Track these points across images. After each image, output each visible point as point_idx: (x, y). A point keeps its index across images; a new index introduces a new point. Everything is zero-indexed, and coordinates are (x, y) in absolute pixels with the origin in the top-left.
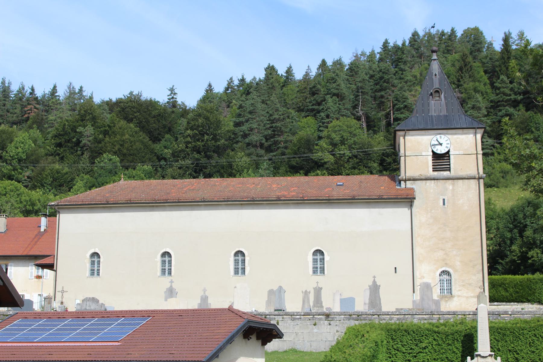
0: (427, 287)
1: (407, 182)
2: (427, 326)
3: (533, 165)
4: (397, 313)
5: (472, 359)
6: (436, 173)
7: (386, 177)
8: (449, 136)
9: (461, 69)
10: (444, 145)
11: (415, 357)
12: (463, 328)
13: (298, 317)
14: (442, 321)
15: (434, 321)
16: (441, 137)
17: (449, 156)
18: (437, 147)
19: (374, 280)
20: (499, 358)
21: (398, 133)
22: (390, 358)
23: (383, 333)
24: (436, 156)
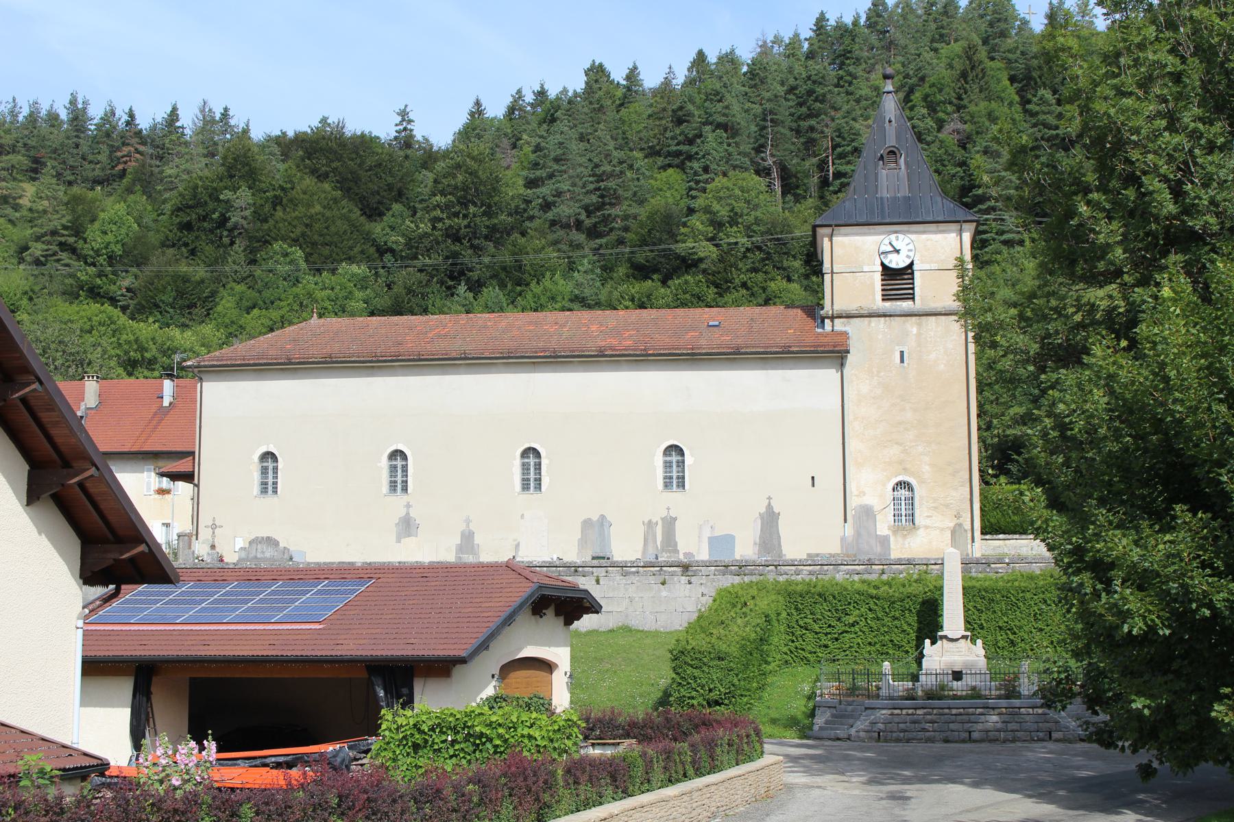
0: (867, 513)
1: (836, 321)
2: (857, 586)
3: (998, 338)
4: (809, 562)
5: (933, 643)
6: (888, 304)
7: (799, 311)
8: (913, 237)
9: (964, 75)
10: (903, 253)
11: (837, 639)
12: (921, 589)
13: (633, 569)
14: (885, 577)
15: (873, 577)
16: (897, 239)
17: (912, 273)
18: (891, 256)
19: (769, 503)
20: (979, 642)
21: (820, 231)
22: (793, 641)
23: (781, 598)
24: (889, 273)
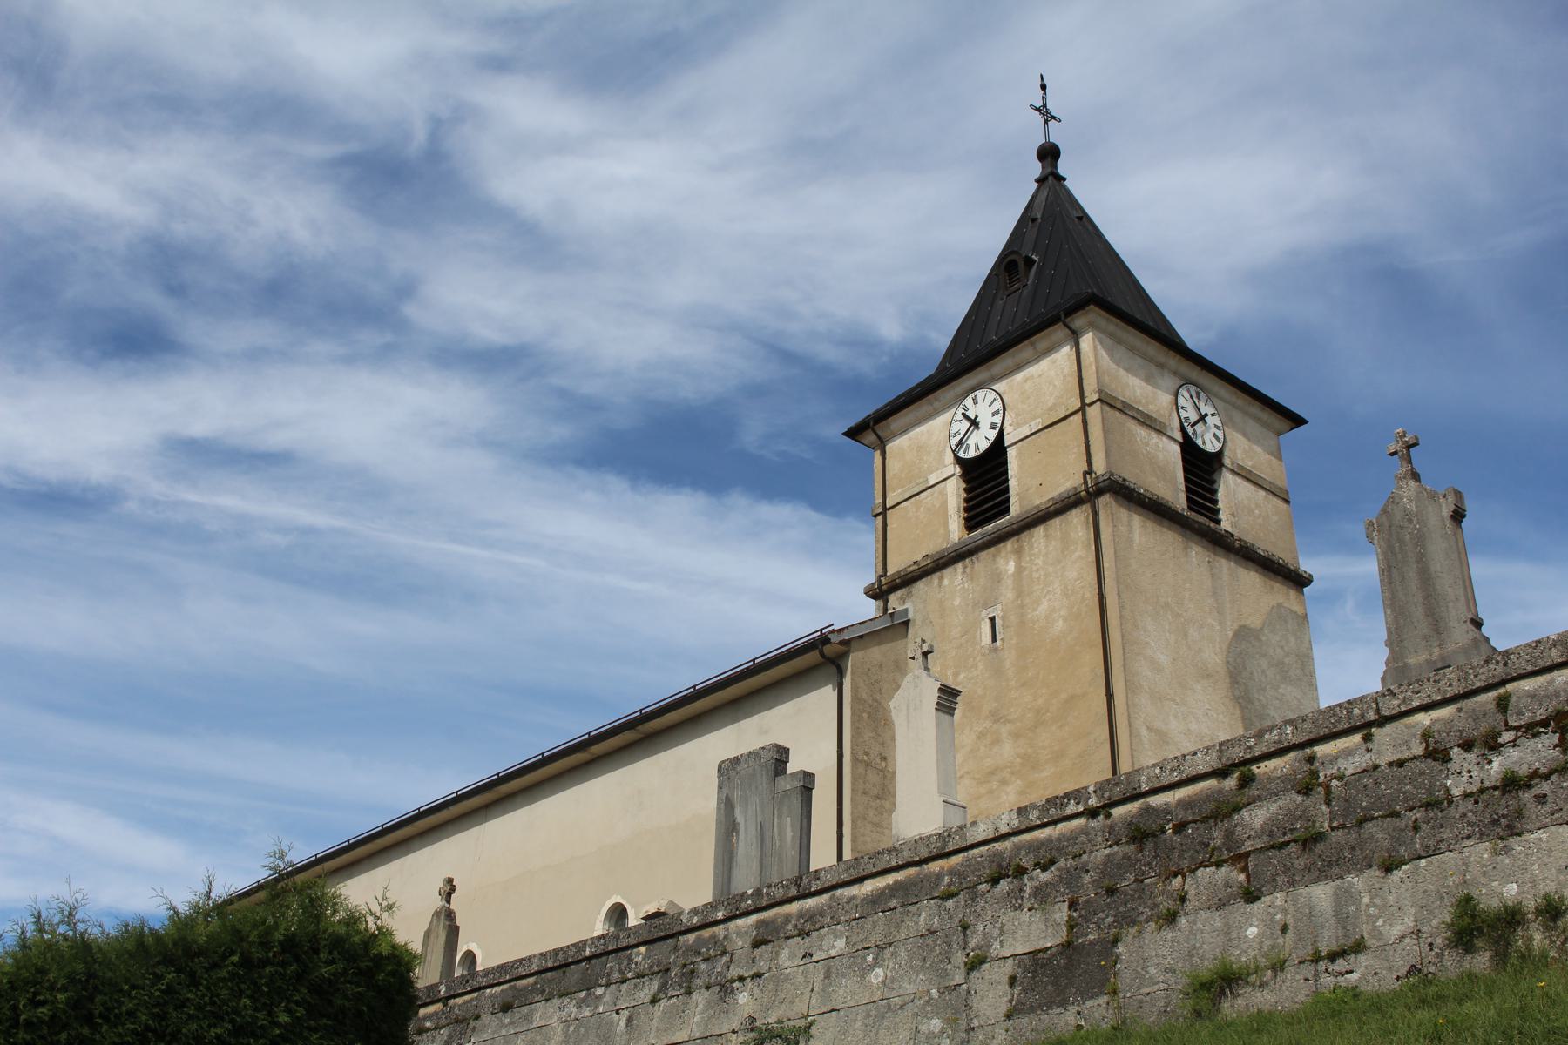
10: (985, 420)
16: (975, 401)
